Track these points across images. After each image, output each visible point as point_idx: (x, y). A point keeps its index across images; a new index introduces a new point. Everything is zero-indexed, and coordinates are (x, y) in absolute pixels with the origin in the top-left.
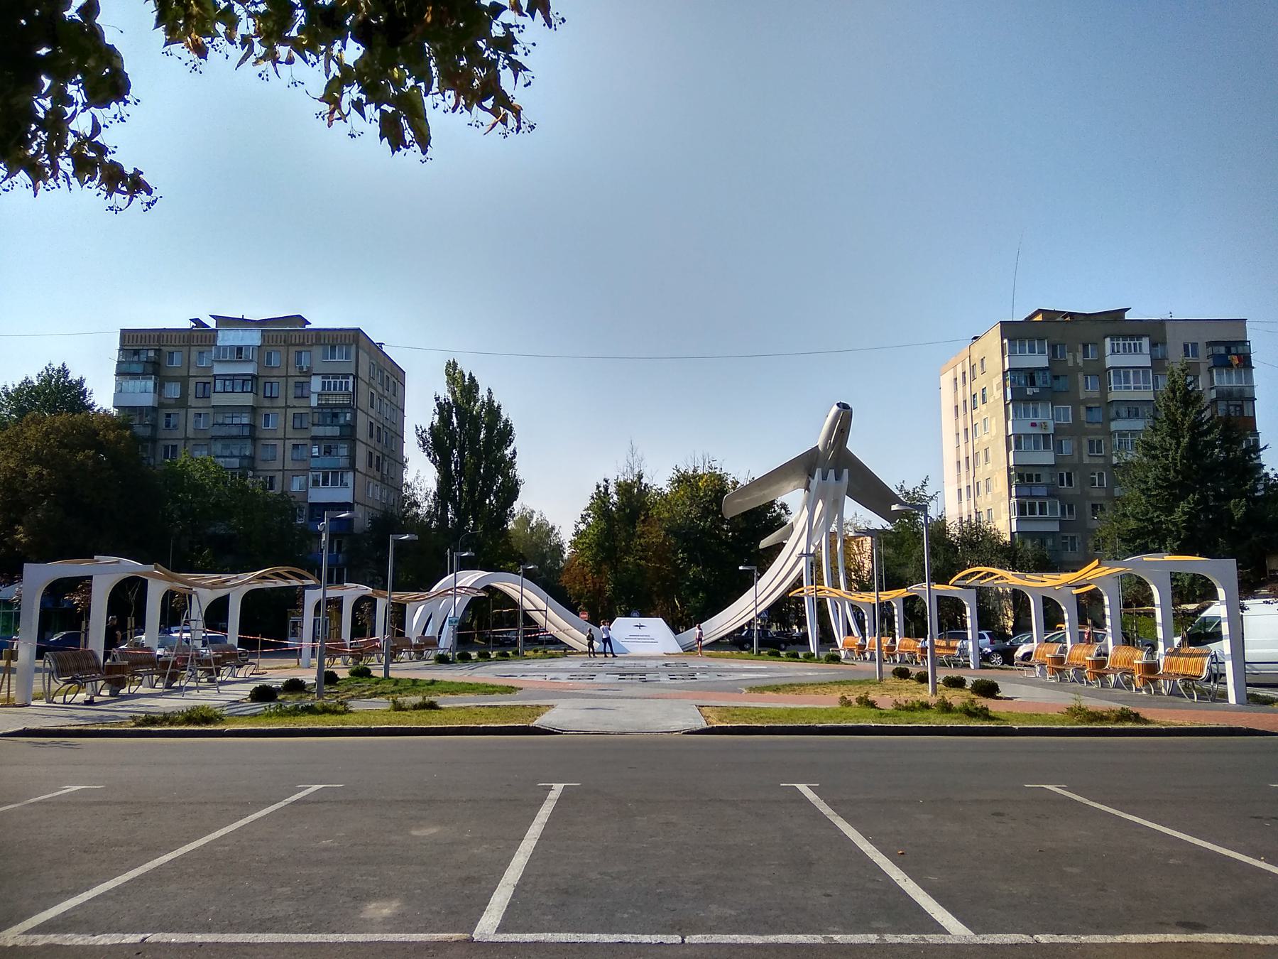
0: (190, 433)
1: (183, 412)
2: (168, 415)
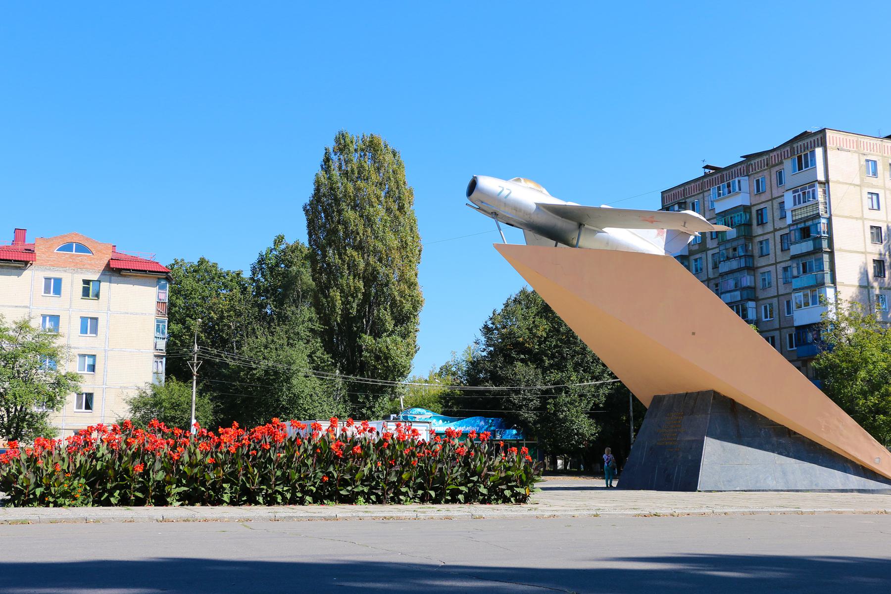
0: (711, 276)
1: (704, 256)
2: (696, 260)
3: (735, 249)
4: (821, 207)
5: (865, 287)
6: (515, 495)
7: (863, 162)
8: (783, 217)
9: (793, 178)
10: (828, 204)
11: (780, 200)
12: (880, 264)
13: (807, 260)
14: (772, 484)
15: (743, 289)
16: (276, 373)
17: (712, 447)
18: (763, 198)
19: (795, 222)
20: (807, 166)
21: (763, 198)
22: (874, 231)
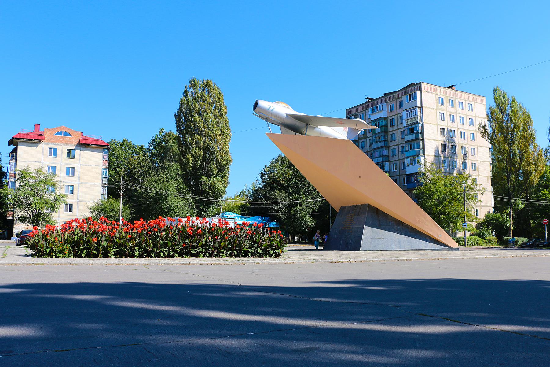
0: (369, 150)
1: (365, 140)
2: (362, 142)
3: (380, 138)
4: (419, 118)
5: (437, 156)
6: (275, 253)
7: (438, 99)
8: (402, 123)
9: (406, 105)
10: (422, 117)
11: (400, 115)
12: (444, 146)
13: (412, 143)
14: (394, 247)
15: (383, 156)
16: (161, 195)
17: (367, 231)
18: (393, 113)
19: (407, 126)
20: (413, 99)
21: (393, 113)
22: (442, 130)
